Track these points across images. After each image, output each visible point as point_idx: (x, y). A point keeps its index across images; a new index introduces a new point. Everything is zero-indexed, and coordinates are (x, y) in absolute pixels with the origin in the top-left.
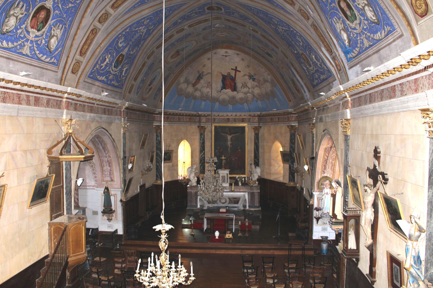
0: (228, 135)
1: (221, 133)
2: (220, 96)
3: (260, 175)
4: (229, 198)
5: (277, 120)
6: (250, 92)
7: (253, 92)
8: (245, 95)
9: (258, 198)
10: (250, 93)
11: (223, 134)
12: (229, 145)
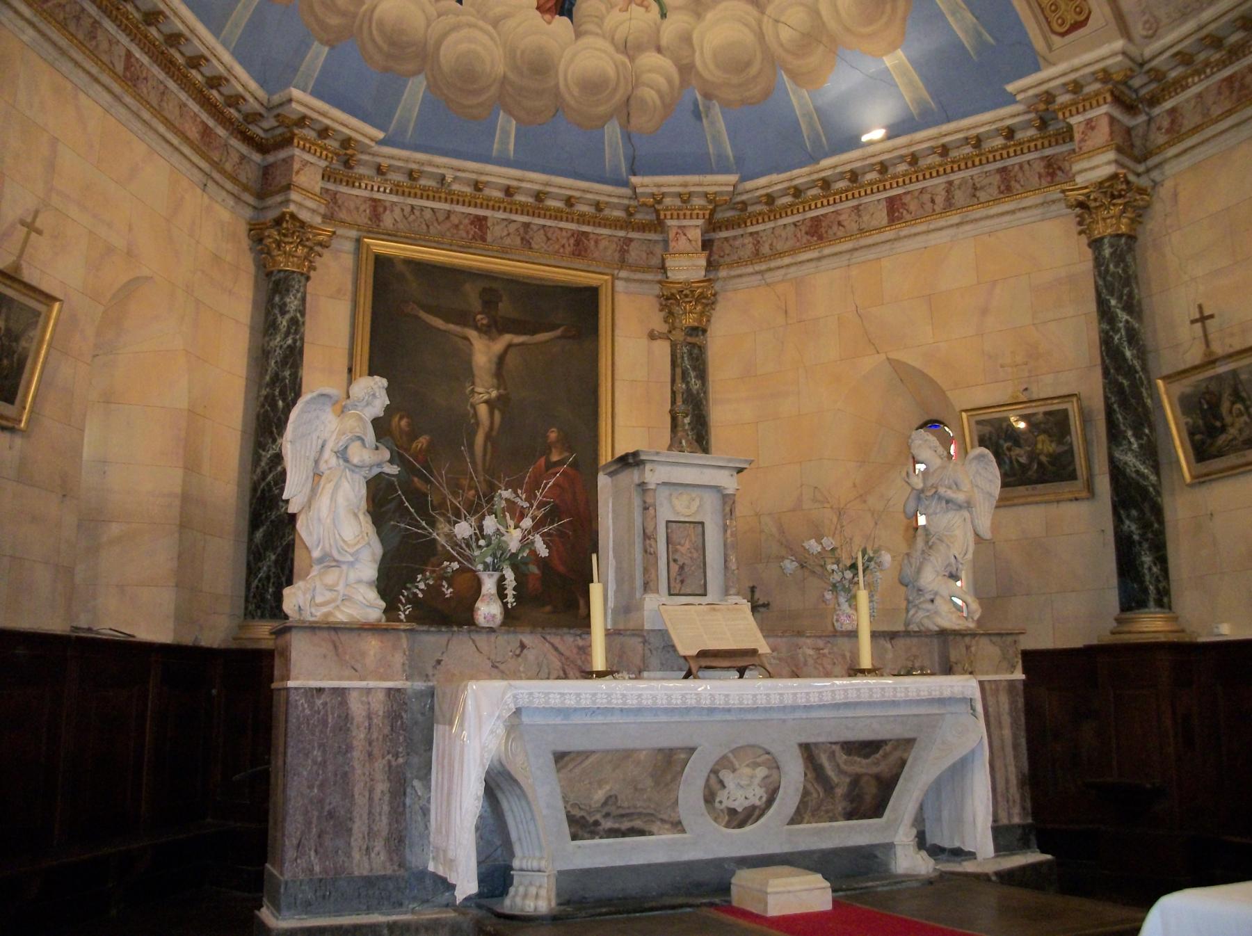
0: (472, 334)
1: (423, 315)
2: (445, 35)
3: (986, 533)
4: (808, 750)
5: (882, 217)
6: (664, 42)
7: (687, 39)
8: (622, 58)
9: (1016, 746)
10: (659, 50)
11: (438, 323)
12: (483, 410)
